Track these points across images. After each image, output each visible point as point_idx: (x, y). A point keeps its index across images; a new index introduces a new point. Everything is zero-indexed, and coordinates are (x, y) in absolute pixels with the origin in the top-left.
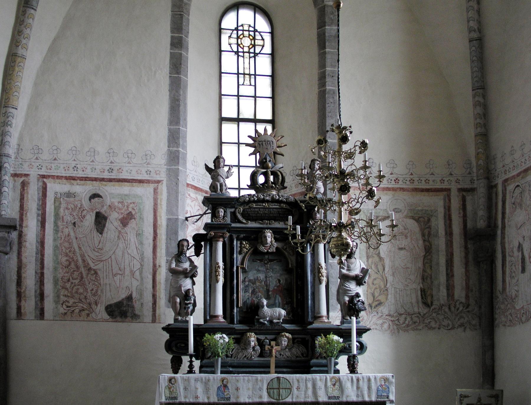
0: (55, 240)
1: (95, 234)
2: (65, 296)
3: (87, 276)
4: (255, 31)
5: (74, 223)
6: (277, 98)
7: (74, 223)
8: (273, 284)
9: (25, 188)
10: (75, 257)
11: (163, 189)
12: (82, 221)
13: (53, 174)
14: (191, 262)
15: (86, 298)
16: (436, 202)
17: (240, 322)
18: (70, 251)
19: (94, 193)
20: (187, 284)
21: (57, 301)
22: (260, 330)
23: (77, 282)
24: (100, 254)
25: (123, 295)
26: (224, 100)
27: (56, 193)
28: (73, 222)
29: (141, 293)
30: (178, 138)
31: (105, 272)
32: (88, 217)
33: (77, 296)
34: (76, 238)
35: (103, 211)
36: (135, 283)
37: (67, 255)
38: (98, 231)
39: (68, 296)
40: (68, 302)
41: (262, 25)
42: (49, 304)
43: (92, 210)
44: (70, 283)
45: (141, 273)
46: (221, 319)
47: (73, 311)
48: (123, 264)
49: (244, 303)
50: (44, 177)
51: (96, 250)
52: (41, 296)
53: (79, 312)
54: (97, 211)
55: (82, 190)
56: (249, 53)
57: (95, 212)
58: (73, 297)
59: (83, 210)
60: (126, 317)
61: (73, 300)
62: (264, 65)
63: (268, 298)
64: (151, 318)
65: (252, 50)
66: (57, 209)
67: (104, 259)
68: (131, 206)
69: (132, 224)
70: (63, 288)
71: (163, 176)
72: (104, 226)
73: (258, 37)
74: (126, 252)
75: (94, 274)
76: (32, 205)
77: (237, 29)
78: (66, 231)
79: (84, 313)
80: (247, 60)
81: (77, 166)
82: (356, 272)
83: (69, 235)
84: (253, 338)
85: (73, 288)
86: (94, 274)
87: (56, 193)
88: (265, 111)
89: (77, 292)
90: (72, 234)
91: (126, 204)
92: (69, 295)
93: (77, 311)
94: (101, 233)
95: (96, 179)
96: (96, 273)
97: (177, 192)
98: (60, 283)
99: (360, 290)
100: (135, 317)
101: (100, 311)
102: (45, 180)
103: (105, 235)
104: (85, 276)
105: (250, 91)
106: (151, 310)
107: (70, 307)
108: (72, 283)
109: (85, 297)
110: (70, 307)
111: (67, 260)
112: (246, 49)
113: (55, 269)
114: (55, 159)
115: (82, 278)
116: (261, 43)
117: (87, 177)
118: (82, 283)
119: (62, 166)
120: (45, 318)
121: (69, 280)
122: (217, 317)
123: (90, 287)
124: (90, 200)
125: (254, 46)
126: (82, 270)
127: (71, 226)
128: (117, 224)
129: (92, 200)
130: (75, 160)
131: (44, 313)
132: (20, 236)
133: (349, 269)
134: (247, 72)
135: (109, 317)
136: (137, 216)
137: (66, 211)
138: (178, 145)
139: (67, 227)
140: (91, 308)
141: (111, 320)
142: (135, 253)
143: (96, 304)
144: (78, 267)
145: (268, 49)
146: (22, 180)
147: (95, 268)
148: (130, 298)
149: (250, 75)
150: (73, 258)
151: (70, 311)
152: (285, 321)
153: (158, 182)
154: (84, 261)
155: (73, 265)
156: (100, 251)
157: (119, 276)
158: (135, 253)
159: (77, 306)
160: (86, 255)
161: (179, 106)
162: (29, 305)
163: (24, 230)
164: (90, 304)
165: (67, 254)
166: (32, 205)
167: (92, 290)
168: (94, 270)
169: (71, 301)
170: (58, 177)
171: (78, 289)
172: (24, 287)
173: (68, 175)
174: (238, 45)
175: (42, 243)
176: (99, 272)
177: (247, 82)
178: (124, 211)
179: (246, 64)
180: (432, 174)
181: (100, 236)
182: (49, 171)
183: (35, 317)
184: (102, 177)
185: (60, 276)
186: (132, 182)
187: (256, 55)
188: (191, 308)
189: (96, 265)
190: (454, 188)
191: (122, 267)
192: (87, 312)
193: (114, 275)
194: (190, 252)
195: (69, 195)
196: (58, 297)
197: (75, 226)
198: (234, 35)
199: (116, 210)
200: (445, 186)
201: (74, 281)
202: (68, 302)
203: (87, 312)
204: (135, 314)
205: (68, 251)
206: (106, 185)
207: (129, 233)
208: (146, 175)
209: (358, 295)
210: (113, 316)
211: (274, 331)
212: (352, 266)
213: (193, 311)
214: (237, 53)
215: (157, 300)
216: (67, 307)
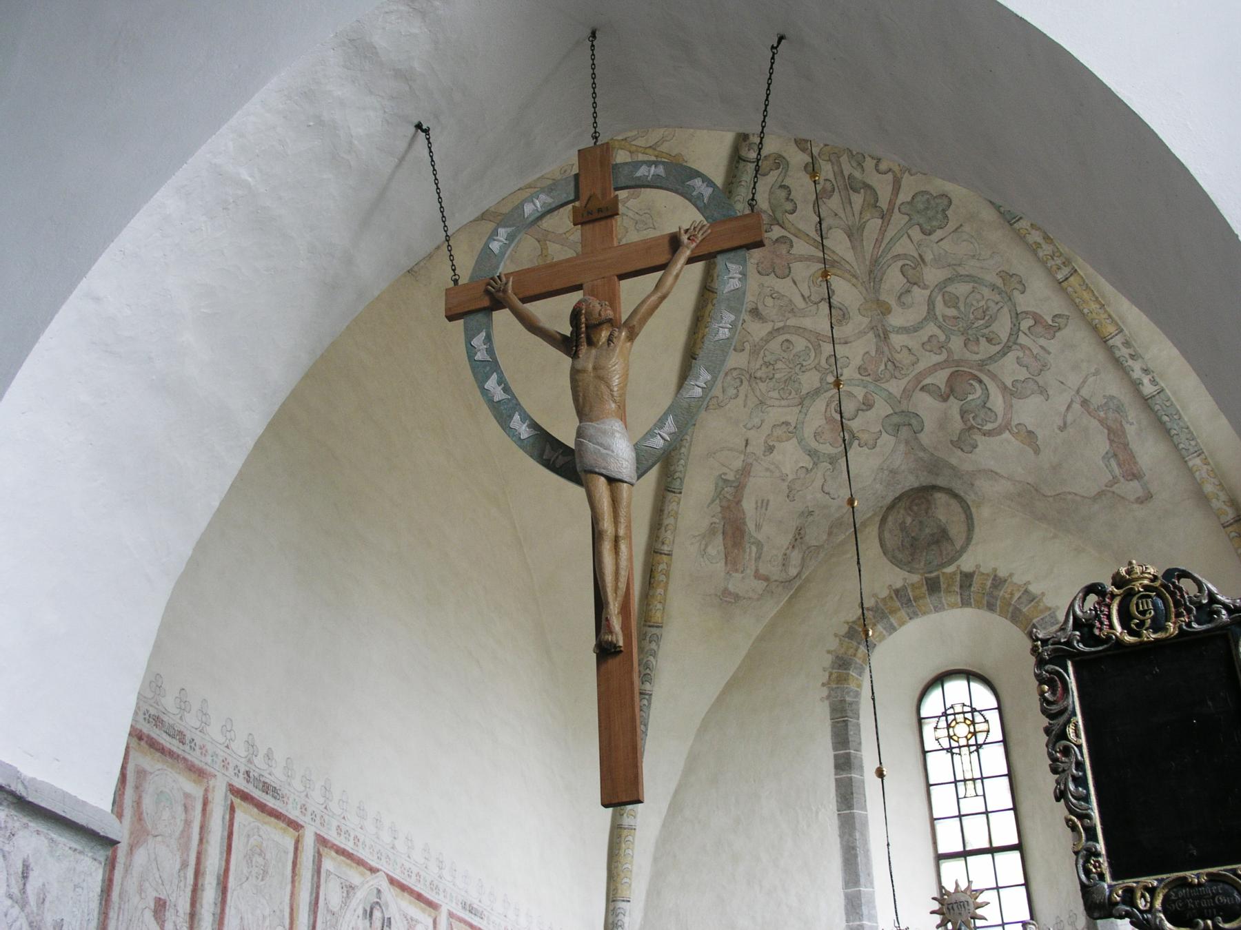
4: (973, 710)
6: (1024, 808)
26: (939, 826)
30: (860, 906)
41: (983, 697)
56: (968, 746)
62: (994, 759)
65: (972, 741)
73: (978, 718)
77: (945, 714)
80: (966, 758)
88: (1006, 832)
105: (976, 805)
112: (963, 742)
116: (983, 727)
125: (975, 734)
134: (968, 776)
138: (861, 917)
145: (996, 734)
149: (974, 780)
161: (856, 856)
174: (950, 737)
177: (971, 792)
179: (966, 764)
187: (979, 746)
198: (943, 724)
214: (950, 750)
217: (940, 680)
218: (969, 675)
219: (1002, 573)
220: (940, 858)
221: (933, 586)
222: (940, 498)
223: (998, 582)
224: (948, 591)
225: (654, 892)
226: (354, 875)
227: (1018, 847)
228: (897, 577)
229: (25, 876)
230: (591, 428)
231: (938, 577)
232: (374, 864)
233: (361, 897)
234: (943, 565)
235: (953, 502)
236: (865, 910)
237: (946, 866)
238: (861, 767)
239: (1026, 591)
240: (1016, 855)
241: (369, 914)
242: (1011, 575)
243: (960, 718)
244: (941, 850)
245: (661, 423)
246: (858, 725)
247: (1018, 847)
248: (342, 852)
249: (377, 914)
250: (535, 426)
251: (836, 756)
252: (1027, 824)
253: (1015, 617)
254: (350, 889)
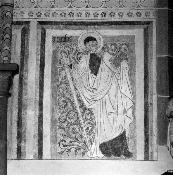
1: (91, 76)
2: (62, 135)
3: (83, 115)
5: (71, 65)
7: (71, 65)
9: (26, 35)
10: (71, 97)
12: (78, 63)
13: (51, 20)
15: (81, 136)
18: (67, 92)
19: (89, 36)
23: (73, 121)
24: (94, 94)
28: (69, 64)
31: (99, 111)
32: (83, 59)
34: (73, 80)
35: (97, 53)
38: (92, 72)
39: (65, 135)
40: (65, 141)
44: (66, 122)
45: (133, 112)
47: (70, 150)
48: (116, 103)
51: (91, 90)
53: (75, 151)
54: (92, 53)
57: (89, 54)
58: (69, 136)
59: (79, 53)
60: (119, 155)
61: (69, 140)
64: (144, 156)
67: (97, 99)
68: (124, 46)
70: (60, 128)
72: (98, 67)
74: (119, 91)
75: (89, 113)
79: (80, 152)
81: (73, 12)
83: (66, 77)
85: (69, 127)
86: (89, 113)
89: (73, 132)
90: (69, 77)
91: (118, 45)
92: (66, 134)
94: (96, 74)
95: (90, 24)
96: (91, 112)
100: (128, 155)
101: (95, 150)
102: (44, 26)
104: (80, 116)
106: (144, 147)
107: (66, 146)
108: (68, 123)
109: (81, 136)
110: (66, 146)
111: (64, 101)
114: (53, 7)
115: (78, 117)
117: (82, 22)
119: (59, 13)
120: (43, 158)
121: (65, 120)
123: (84, 126)
124: (85, 43)
127: (67, 70)
129: (87, 43)
130: (70, 6)
131: (42, 153)
135: (103, 155)
137: (63, 54)
139: (64, 70)
140: (86, 146)
141: (106, 158)
143: (91, 142)
144: (74, 107)
146: (22, 27)
147: (90, 107)
150: (69, 99)
151: (66, 150)
154: (80, 101)
156: (95, 91)
157: (112, 114)
159: (73, 145)
160: (82, 95)
163: (24, 73)
164: (85, 143)
165: (64, 94)
167: (88, 129)
168: (89, 110)
169: (68, 140)
170: (57, 23)
171: (74, 128)
172: (24, 128)
173: (64, 21)
176: (94, 112)
181: (95, 76)
182: (47, 18)
183: (34, 156)
184: (96, 21)
185: (57, 117)
186: (123, 25)
189: (91, 105)
191: (115, 106)
192: (82, 150)
196: (56, 137)
197: (71, 68)
199: (109, 51)
201: (70, 121)
202: (65, 141)
203: (82, 150)
204: (128, 152)
205: (65, 92)
206: (99, 29)
207: (121, 73)
208: (136, 17)
210: (107, 154)
215: (150, 137)
216: (64, 146)
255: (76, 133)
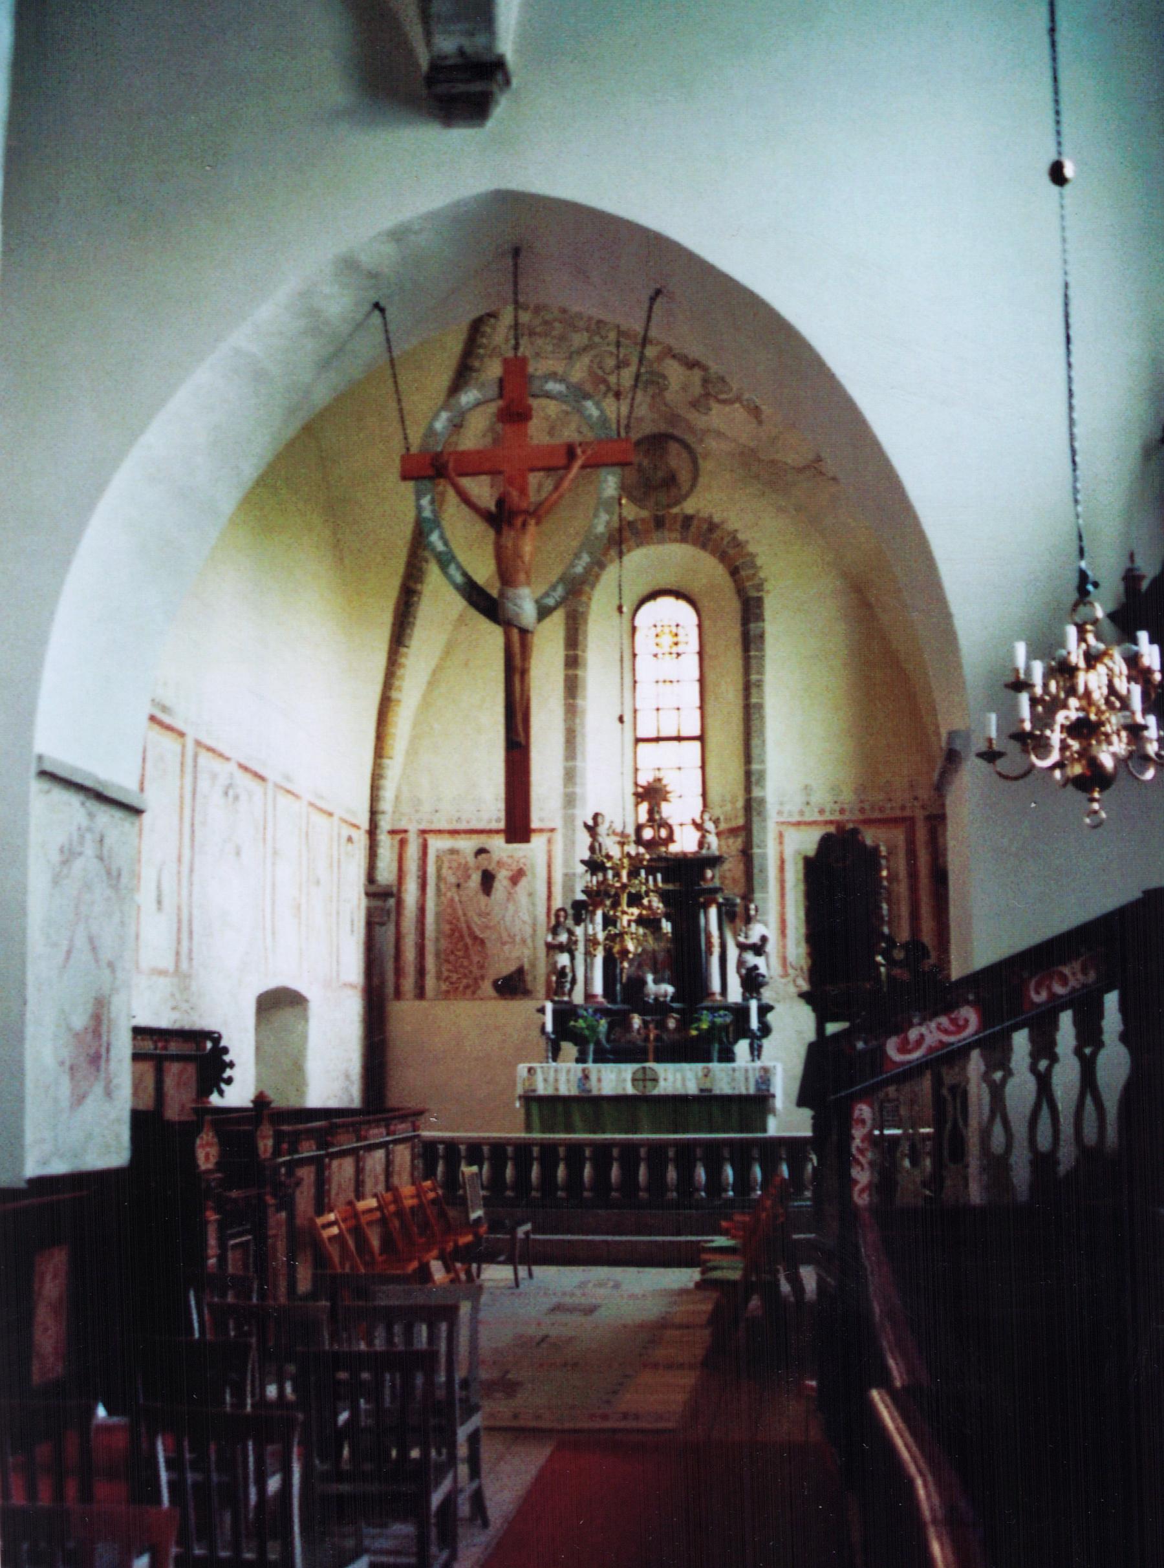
0: (437, 905)
1: (483, 898)
6: (709, 708)
8: (661, 956)
11: (558, 838)
14: (571, 933)
16: (899, 836)
17: (624, 1001)
20: (563, 959)
21: (439, 977)
22: (644, 1008)
25: (512, 968)
27: (438, 850)
29: (533, 965)
33: (462, 970)
35: (490, 868)
36: (527, 952)
37: (451, 923)
42: (430, 982)
43: (478, 868)
45: (533, 941)
46: (601, 999)
49: (629, 978)
50: (424, 832)
52: (421, 972)
55: (467, 845)
58: (456, 972)
63: (655, 972)
66: (439, 870)
69: (523, 882)
71: (557, 822)
76: (412, 866)
78: (449, 894)
79: (469, 992)
82: (754, 939)
84: (637, 1021)
87: (438, 850)
90: (457, 899)
93: (461, 989)
97: (573, 843)
98: (443, 956)
99: (760, 961)
101: (487, 987)
103: (493, 897)
112: (667, 650)
113: (437, 940)
118: (467, 956)
122: (595, 996)
123: (476, 959)
126: (469, 941)
127: (454, 889)
128: (506, 883)
132: (399, 903)
133: (746, 937)
136: (528, 873)
138: (574, 784)
142: (526, 918)
143: (483, 977)
144: (462, 937)
145: (694, 646)
148: (520, 971)
152: (673, 999)
153: (552, 830)
155: (457, 934)
158: (526, 918)
161: (574, 737)
162: (408, 984)
166: (412, 866)
169: (455, 977)
170: (440, 832)
175: (422, 910)
178: (515, 867)
180: (890, 800)
188: (568, 986)
190: (920, 814)
193: (504, 944)
194: (570, 922)
195: (453, 851)
200: (908, 813)
209: (756, 967)
211: (660, 1008)
212: (750, 933)
213: (571, 990)
217: (653, 595)
218: (678, 594)
219: (716, 519)
220: (638, 740)
221: (659, 523)
222: (674, 447)
223: (712, 527)
224: (670, 530)
225: (412, 751)
226: (217, 765)
227: (701, 738)
228: (631, 511)
229: (101, 841)
230: (510, 592)
231: (663, 516)
232: (227, 753)
233: (223, 781)
234: (669, 506)
235: (685, 455)
236: (578, 780)
237: (641, 745)
238: (585, 665)
239: (734, 538)
240: (697, 744)
241: (226, 794)
242: (723, 523)
243: (667, 630)
244: (640, 735)
245: (553, 588)
246: (585, 632)
247: (701, 738)
248: (210, 749)
249: (231, 793)
250: (465, 574)
251: (567, 656)
252: (709, 721)
253: (723, 557)
254: (214, 777)
255: (466, 968)
